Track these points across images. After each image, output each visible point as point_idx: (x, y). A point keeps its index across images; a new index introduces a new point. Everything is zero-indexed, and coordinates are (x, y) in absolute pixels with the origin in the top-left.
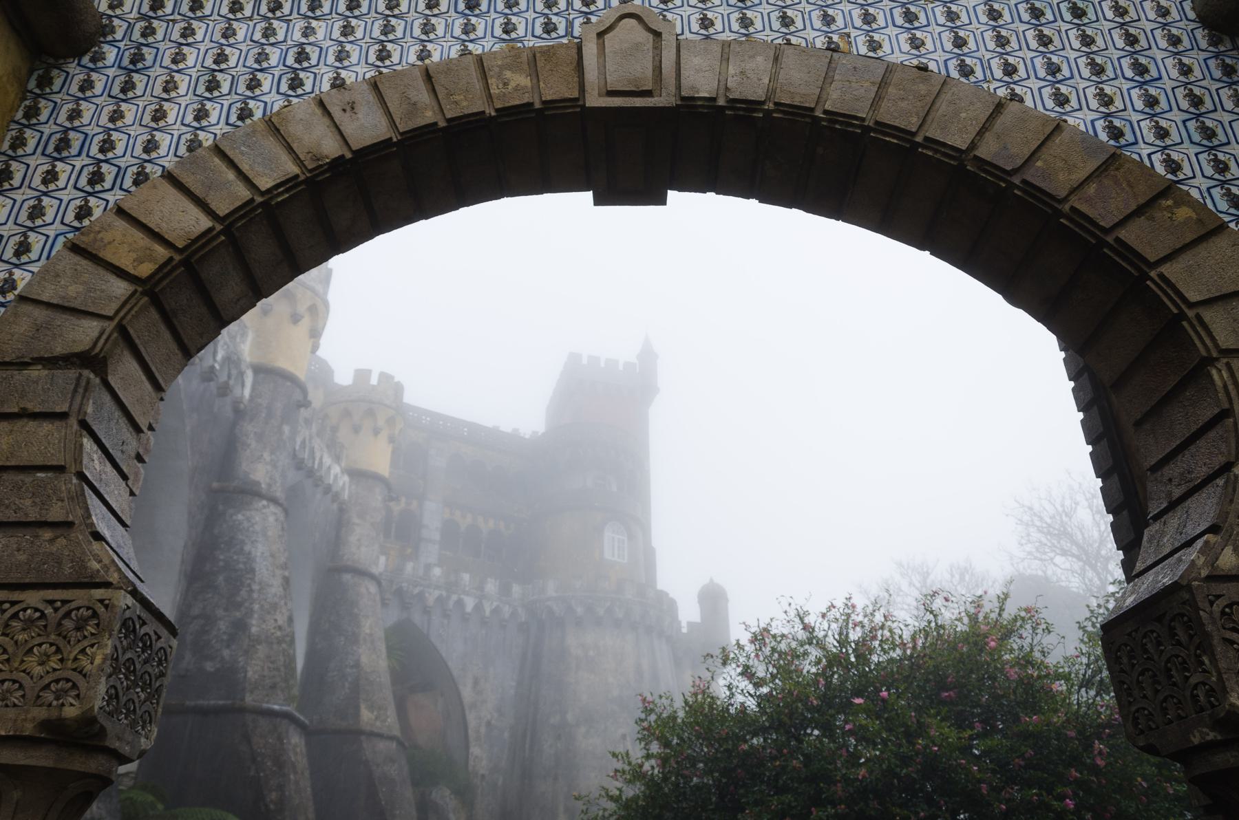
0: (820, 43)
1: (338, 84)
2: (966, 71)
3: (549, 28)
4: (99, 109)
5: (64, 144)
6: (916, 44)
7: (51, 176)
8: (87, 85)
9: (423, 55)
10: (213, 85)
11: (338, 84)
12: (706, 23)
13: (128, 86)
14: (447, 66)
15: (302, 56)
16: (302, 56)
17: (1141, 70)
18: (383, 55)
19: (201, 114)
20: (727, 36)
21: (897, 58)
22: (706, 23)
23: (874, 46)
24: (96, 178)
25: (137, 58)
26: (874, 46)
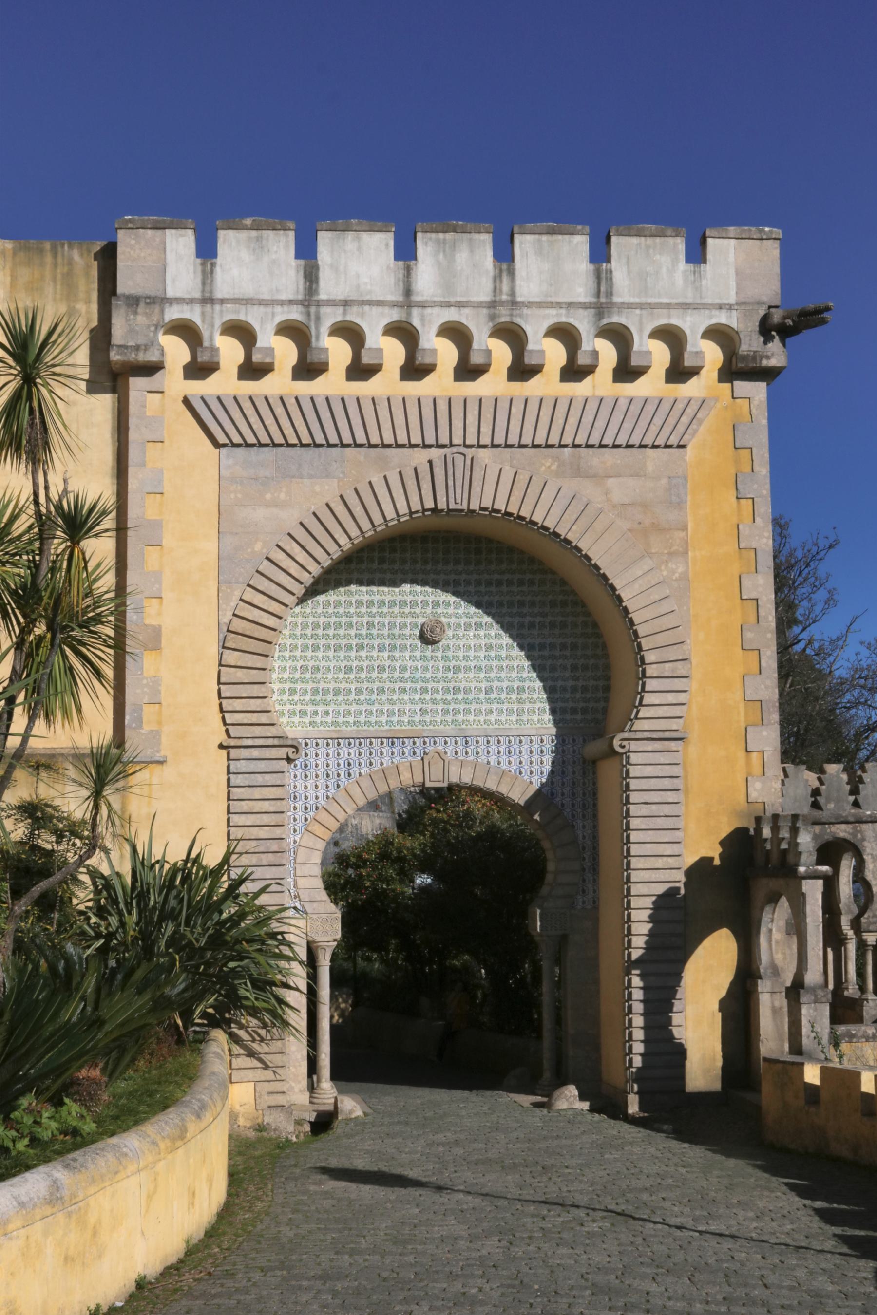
0: (485, 761)
1: (360, 774)
2: (520, 773)
3: (414, 753)
4: (301, 784)
5: (295, 797)
6: (510, 763)
7: (295, 808)
8: (295, 776)
9: (382, 764)
10: (328, 776)
11: (360, 774)
12: (456, 753)
13: (306, 776)
14: (388, 768)
15: (349, 764)
16: (349, 764)
17: (563, 773)
18: (371, 764)
19: (327, 787)
20: (462, 758)
21: (504, 767)
22: (456, 753)
23: (499, 763)
24: (306, 808)
25: (306, 766)
26: (499, 763)
